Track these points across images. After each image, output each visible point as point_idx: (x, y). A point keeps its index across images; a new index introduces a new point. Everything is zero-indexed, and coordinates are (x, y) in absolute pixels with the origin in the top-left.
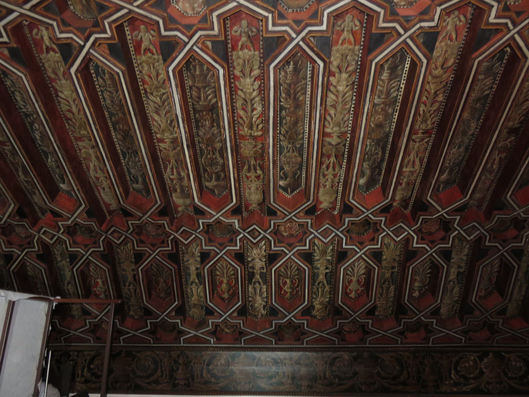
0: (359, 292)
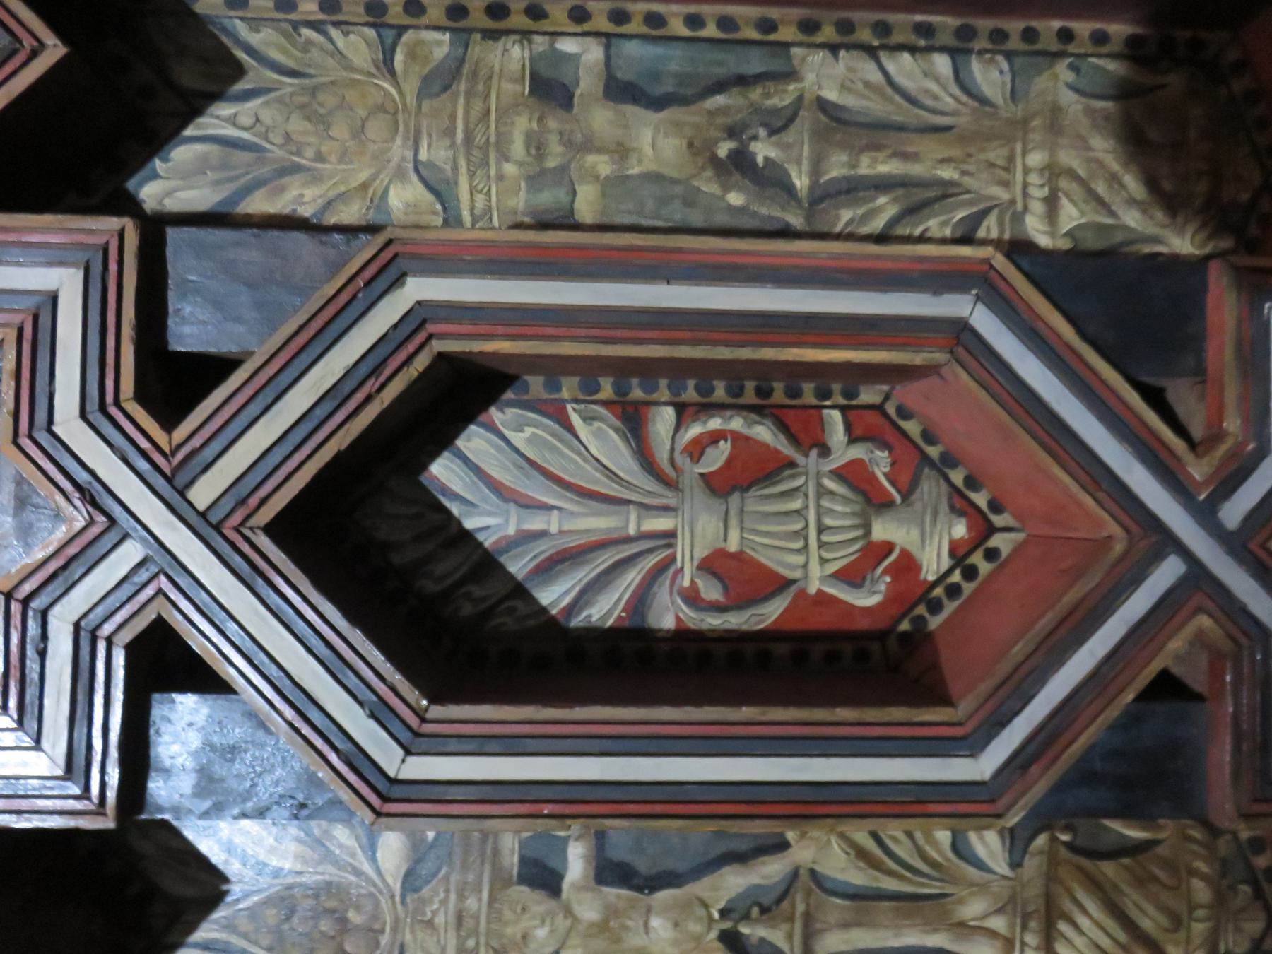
0: (880, 462)
